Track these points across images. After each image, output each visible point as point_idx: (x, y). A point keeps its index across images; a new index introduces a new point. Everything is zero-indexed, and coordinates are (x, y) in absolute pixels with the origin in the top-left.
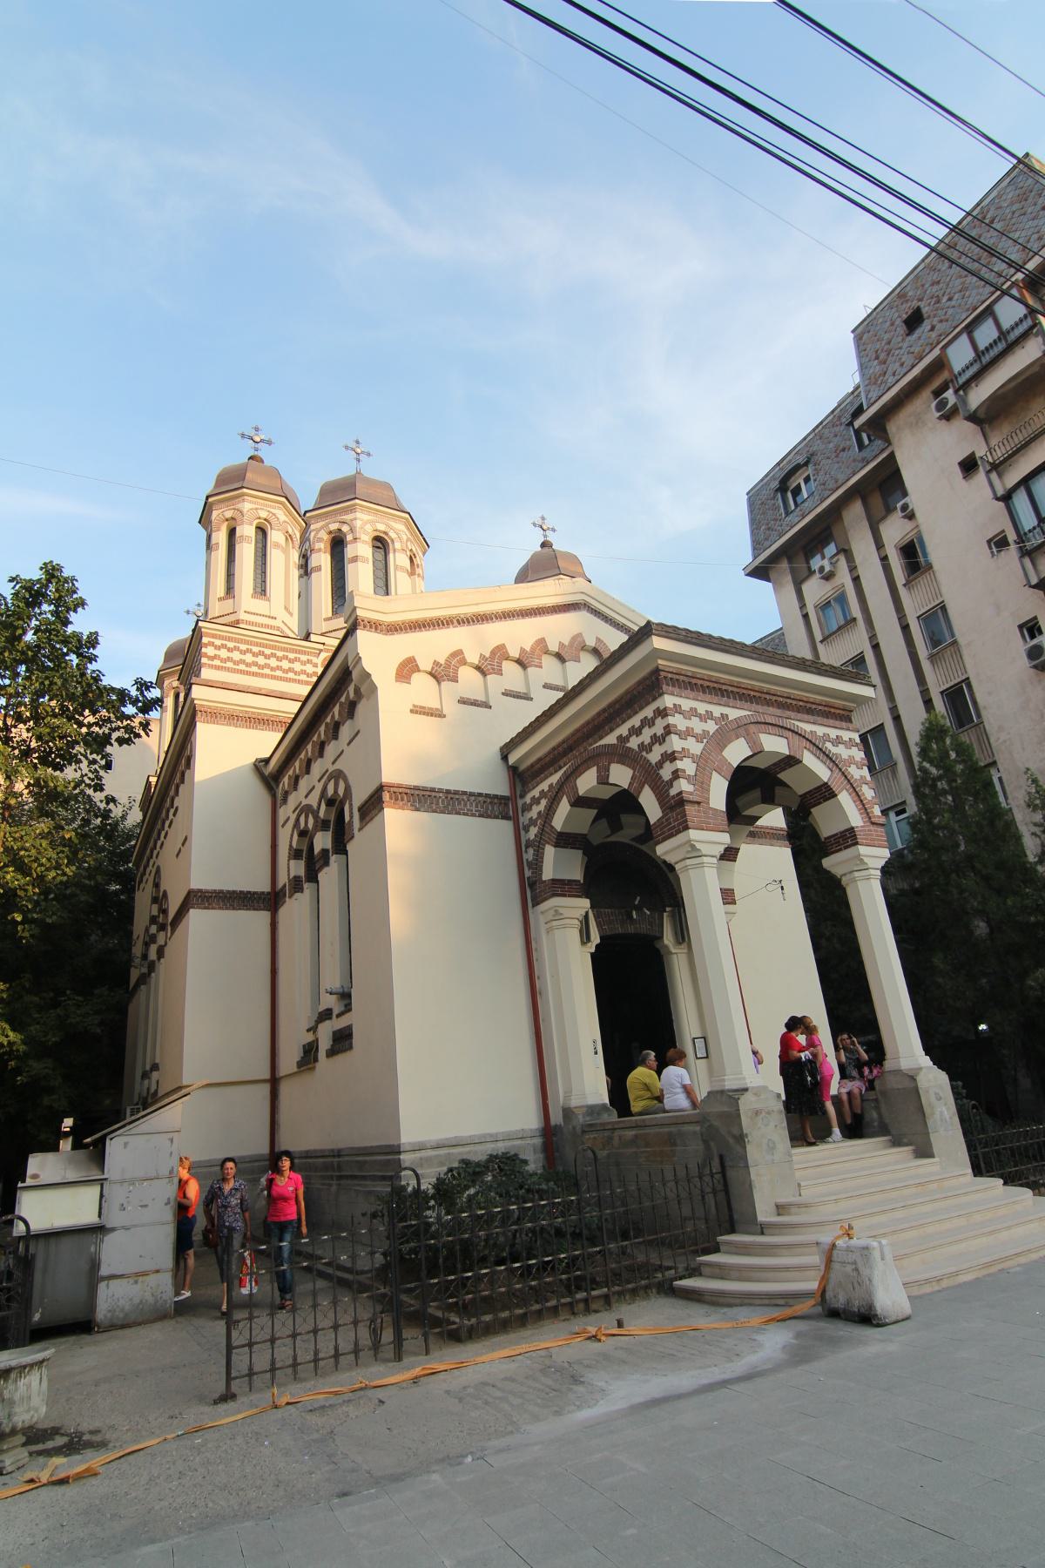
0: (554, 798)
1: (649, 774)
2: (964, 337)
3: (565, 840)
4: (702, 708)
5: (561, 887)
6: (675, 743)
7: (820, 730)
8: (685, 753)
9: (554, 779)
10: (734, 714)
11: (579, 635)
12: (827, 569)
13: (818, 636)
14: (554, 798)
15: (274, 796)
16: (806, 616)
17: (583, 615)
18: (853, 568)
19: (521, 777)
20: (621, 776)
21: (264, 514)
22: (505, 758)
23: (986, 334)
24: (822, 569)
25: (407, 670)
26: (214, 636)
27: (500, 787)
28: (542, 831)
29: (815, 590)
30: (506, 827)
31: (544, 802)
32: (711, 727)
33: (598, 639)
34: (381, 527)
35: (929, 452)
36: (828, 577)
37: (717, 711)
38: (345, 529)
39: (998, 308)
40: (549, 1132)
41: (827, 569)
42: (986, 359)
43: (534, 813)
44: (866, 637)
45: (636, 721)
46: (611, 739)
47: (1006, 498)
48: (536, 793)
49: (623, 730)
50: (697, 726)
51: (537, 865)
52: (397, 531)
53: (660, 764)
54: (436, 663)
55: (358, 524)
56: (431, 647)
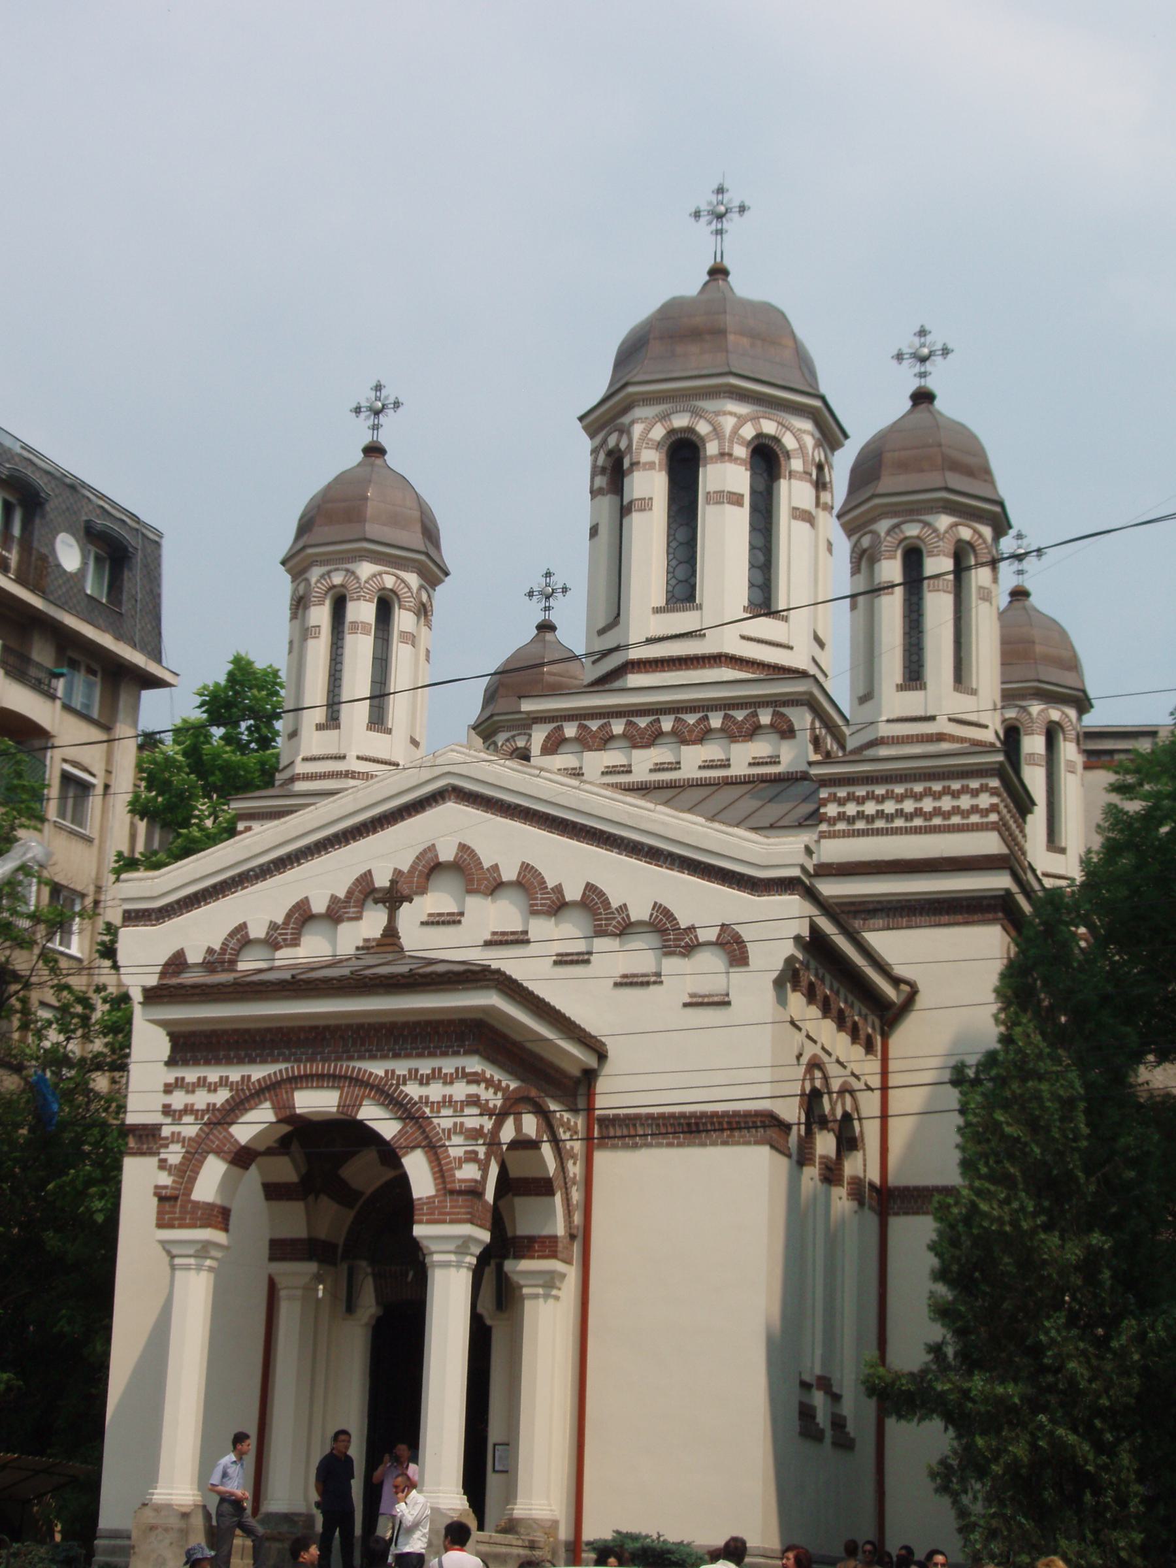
4: (213, 1074)
7: (401, 1067)
8: (176, 1138)
10: (258, 1073)
17: (451, 808)
32: (222, 1096)
33: (463, 848)
37: (235, 1074)
50: (201, 1099)
54: (210, 951)
55: (637, 430)
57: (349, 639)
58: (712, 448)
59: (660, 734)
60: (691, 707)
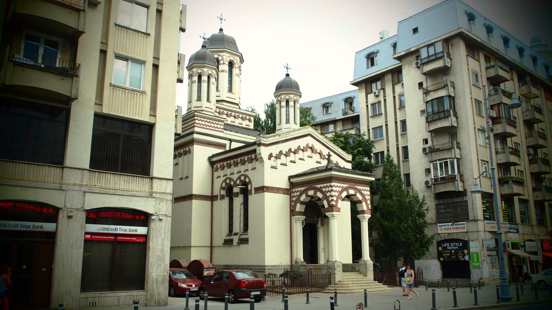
0: (302, 193)
1: (326, 198)
2: (426, 48)
3: (302, 203)
4: (339, 185)
5: (300, 213)
6: (333, 193)
7: (361, 188)
8: (335, 196)
9: (303, 189)
10: (345, 186)
11: (308, 144)
12: (377, 94)
13: (370, 115)
14: (302, 193)
15: (213, 168)
16: (367, 106)
17: (309, 137)
18: (385, 96)
19: (293, 185)
20: (320, 195)
21: (210, 72)
22: (289, 180)
23: (432, 51)
24: (375, 93)
25: (270, 156)
26: (198, 117)
27: (288, 187)
28: (297, 200)
29: (372, 98)
30: (288, 196)
31: (298, 193)
32: (340, 189)
34: (232, 59)
35: (411, 76)
36: (377, 96)
37: (342, 185)
38: (220, 58)
39: (436, 44)
40: (292, 266)
41: (377, 94)
42: (430, 59)
43: (295, 194)
44: (384, 121)
45: (325, 185)
46: (319, 186)
47: (427, 102)
48: (297, 190)
49: (322, 186)
50: (338, 189)
51: (295, 206)
52: (236, 60)
53: (329, 197)
55: (225, 57)
56: (275, 150)
57: (202, 84)
58: (237, 66)
59: (232, 115)
60: (230, 111)
